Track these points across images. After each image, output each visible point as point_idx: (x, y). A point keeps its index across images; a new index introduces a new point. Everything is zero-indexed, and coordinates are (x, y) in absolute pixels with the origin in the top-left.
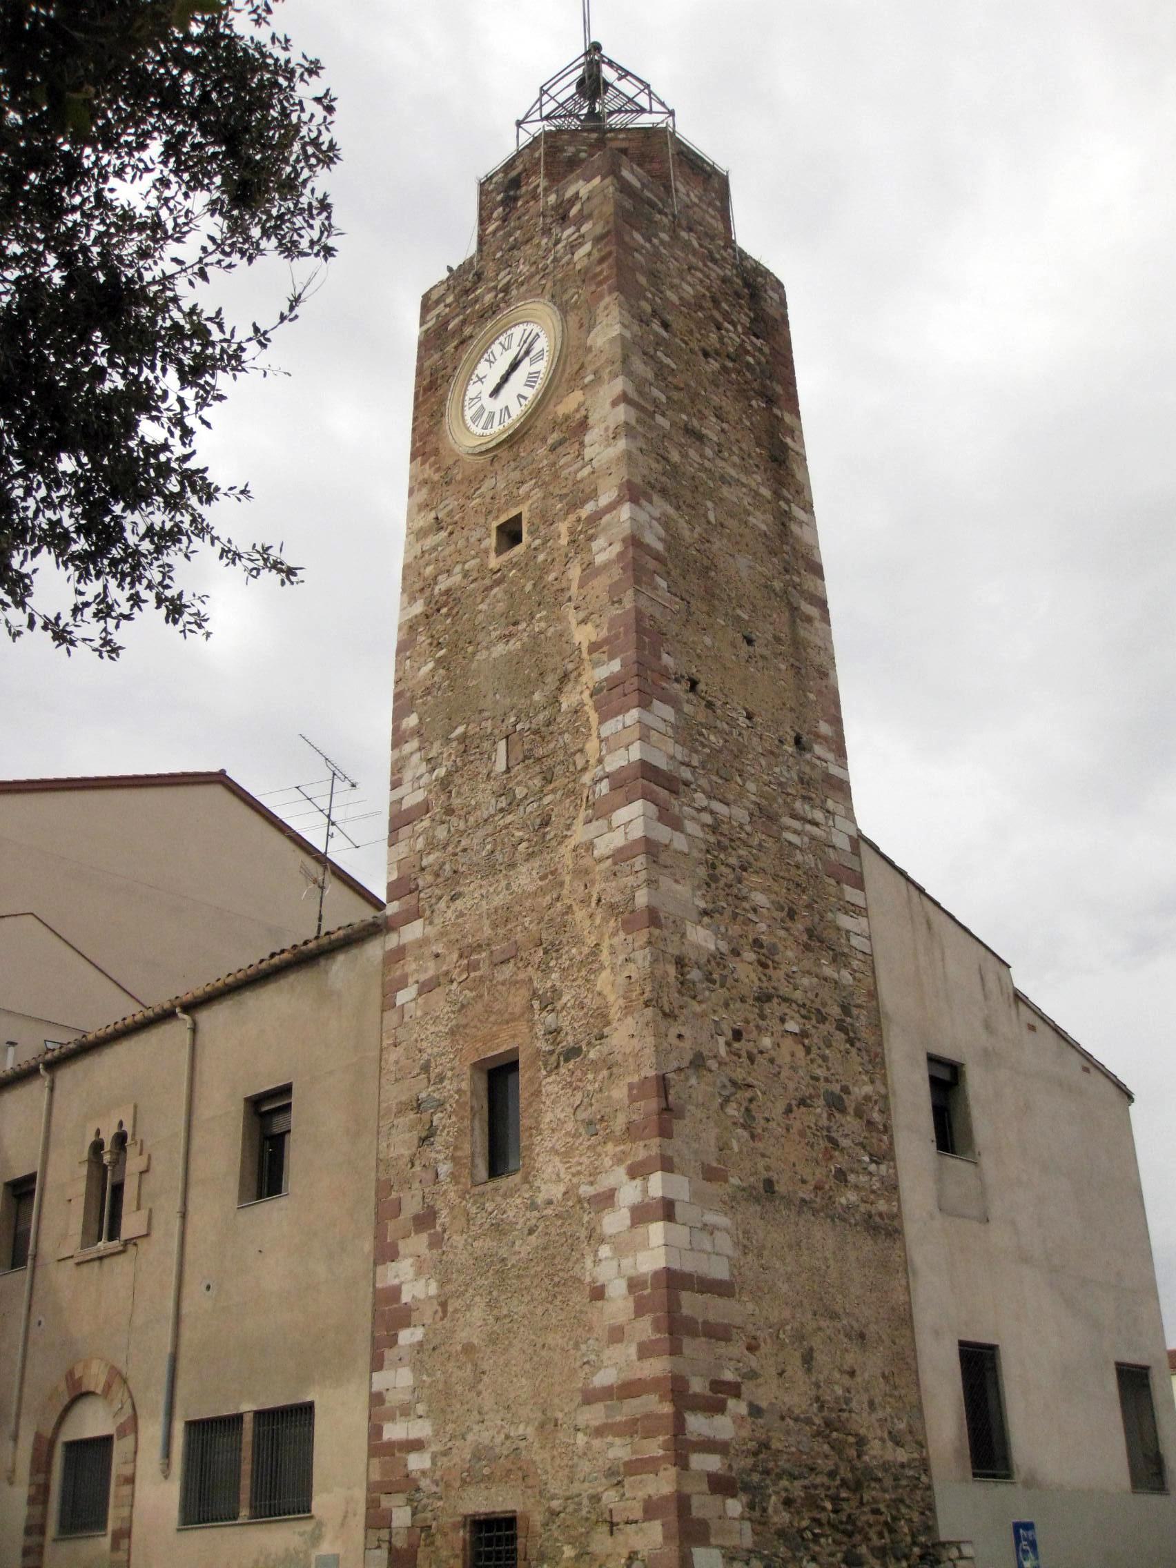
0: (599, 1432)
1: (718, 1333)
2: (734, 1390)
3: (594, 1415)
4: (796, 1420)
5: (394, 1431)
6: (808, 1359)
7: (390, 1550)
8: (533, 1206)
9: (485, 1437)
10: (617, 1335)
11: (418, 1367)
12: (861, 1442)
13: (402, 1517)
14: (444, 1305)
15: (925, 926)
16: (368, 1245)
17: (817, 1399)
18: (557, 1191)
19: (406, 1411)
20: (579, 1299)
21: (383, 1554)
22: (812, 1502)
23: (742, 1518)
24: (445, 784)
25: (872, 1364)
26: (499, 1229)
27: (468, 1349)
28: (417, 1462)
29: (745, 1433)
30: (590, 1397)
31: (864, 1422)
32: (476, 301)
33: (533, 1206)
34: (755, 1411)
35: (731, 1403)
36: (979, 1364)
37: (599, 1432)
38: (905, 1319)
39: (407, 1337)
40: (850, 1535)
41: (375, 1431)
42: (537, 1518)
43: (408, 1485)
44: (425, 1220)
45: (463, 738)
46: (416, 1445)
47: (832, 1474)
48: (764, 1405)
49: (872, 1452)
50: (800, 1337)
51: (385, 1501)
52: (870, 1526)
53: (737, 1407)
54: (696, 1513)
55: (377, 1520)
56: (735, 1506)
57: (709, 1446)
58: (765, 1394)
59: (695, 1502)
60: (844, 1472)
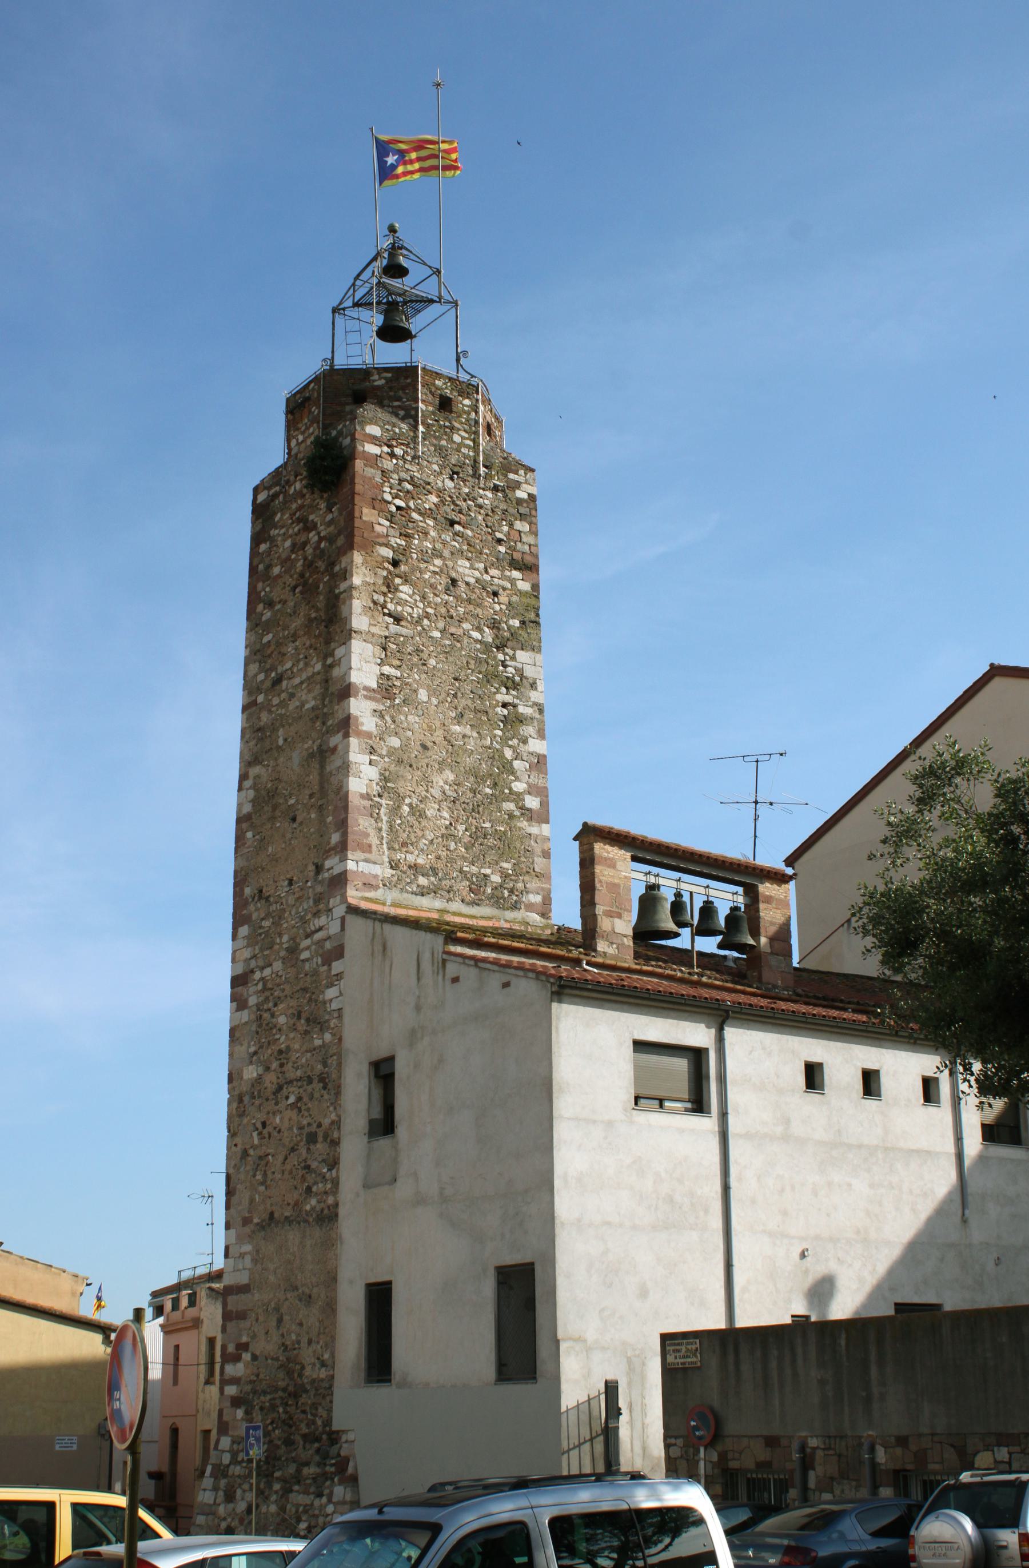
1: (242, 1316)
2: (244, 1347)
4: (273, 1359)
6: (280, 1321)
12: (303, 1368)
15: (381, 948)
17: (283, 1344)
22: (273, 1407)
23: (242, 1419)
25: (312, 1317)
29: (248, 1372)
31: (307, 1355)
34: (255, 1357)
35: (244, 1355)
36: (379, 1298)
38: (332, 1280)
40: (290, 1427)
47: (284, 1390)
48: (258, 1353)
49: (307, 1374)
50: (277, 1309)
52: (301, 1421)
53: (246, 1356)
54: (225, 1418)
56: (240, 1413)
57: (235, 1381)
58: (260, 1346)
59: (225, 1412)
60: (291, 1388)
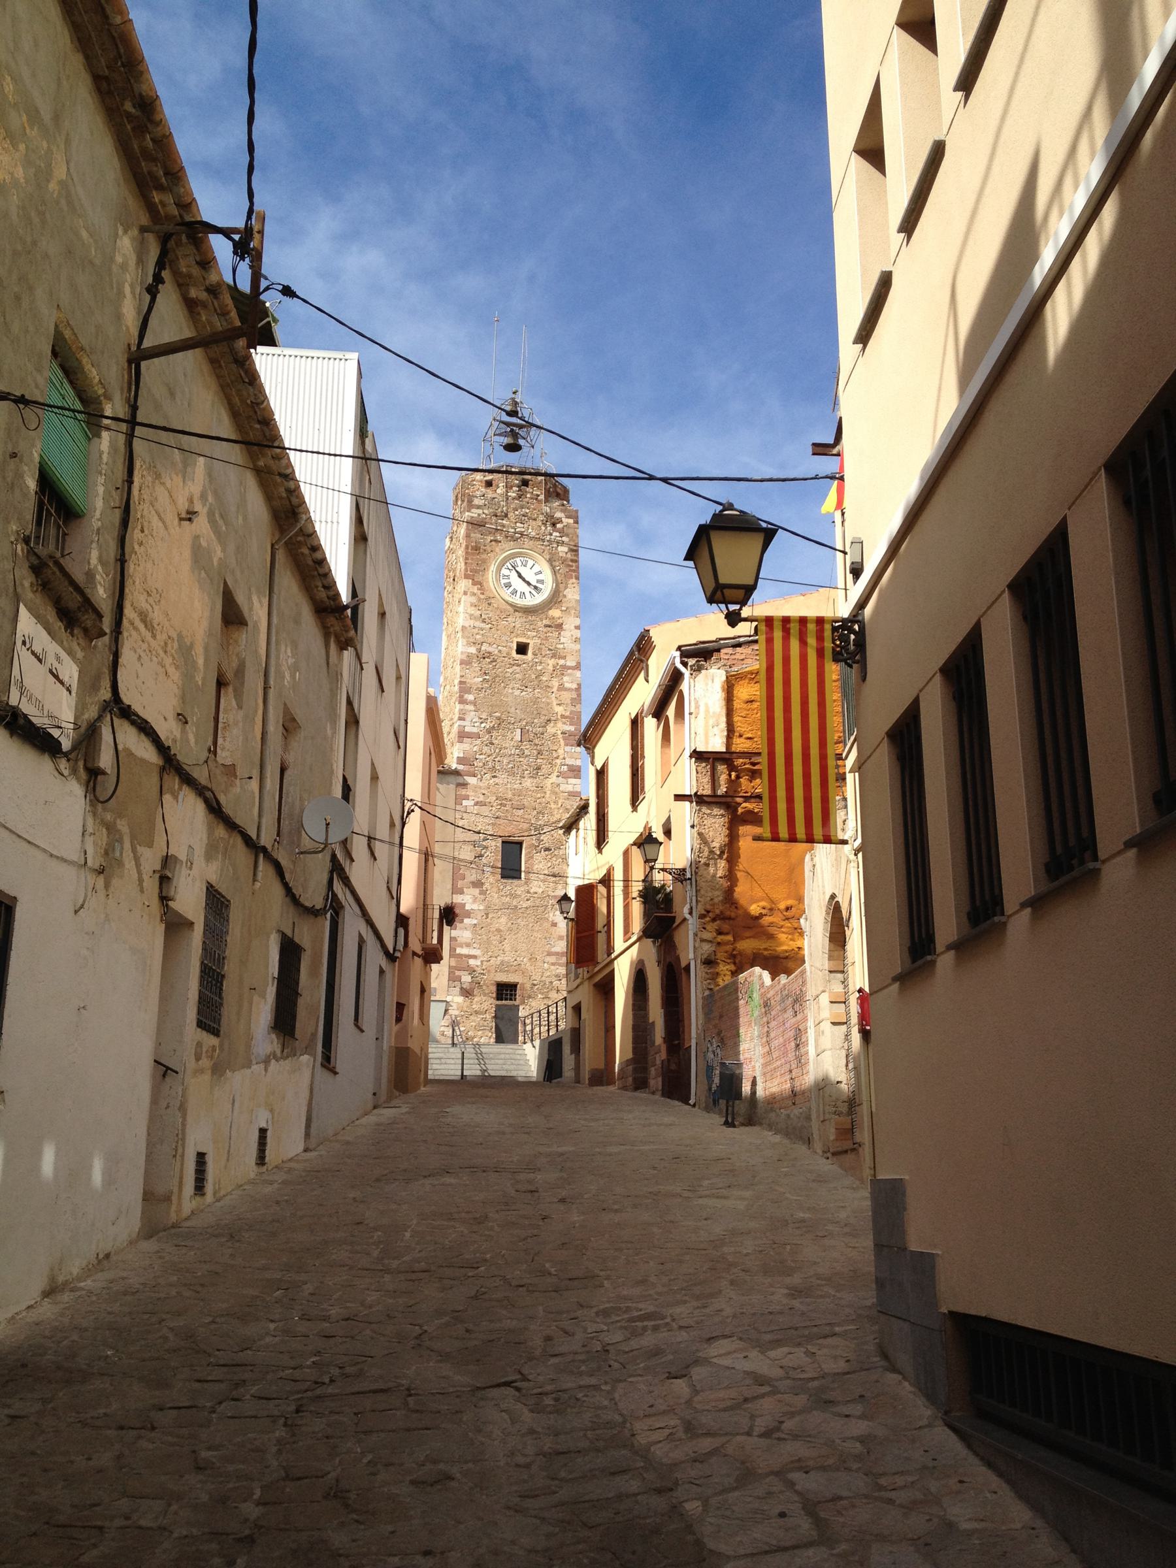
0: (553, 964)
3: (552, 959)
5: (459, 951)
7: (462, 988)
8: (528, 892)
9: (506, 959)
10: (560, 938)
11: (474, 932)
13: (466, 978)
14: (487, 914)
16: (450, 886)
18: (540, 891)
19: (468, 945)
20: (546, 925)
21: (458, 989)
24: (489, 731)
26: (513, 896)
27: (499, 930)
28: (472, 962)
30: (550, 954)
32: (504, 526)
33: (528, 892)
37: (553, 964)
39: (466, 921)
41: (452, 949)
42: (528, 986)
43: (472, 971)
44: (478, 884)
45: (499, 718)
46: (475, 957)
51: (457, 973)
55: (453, 978)
